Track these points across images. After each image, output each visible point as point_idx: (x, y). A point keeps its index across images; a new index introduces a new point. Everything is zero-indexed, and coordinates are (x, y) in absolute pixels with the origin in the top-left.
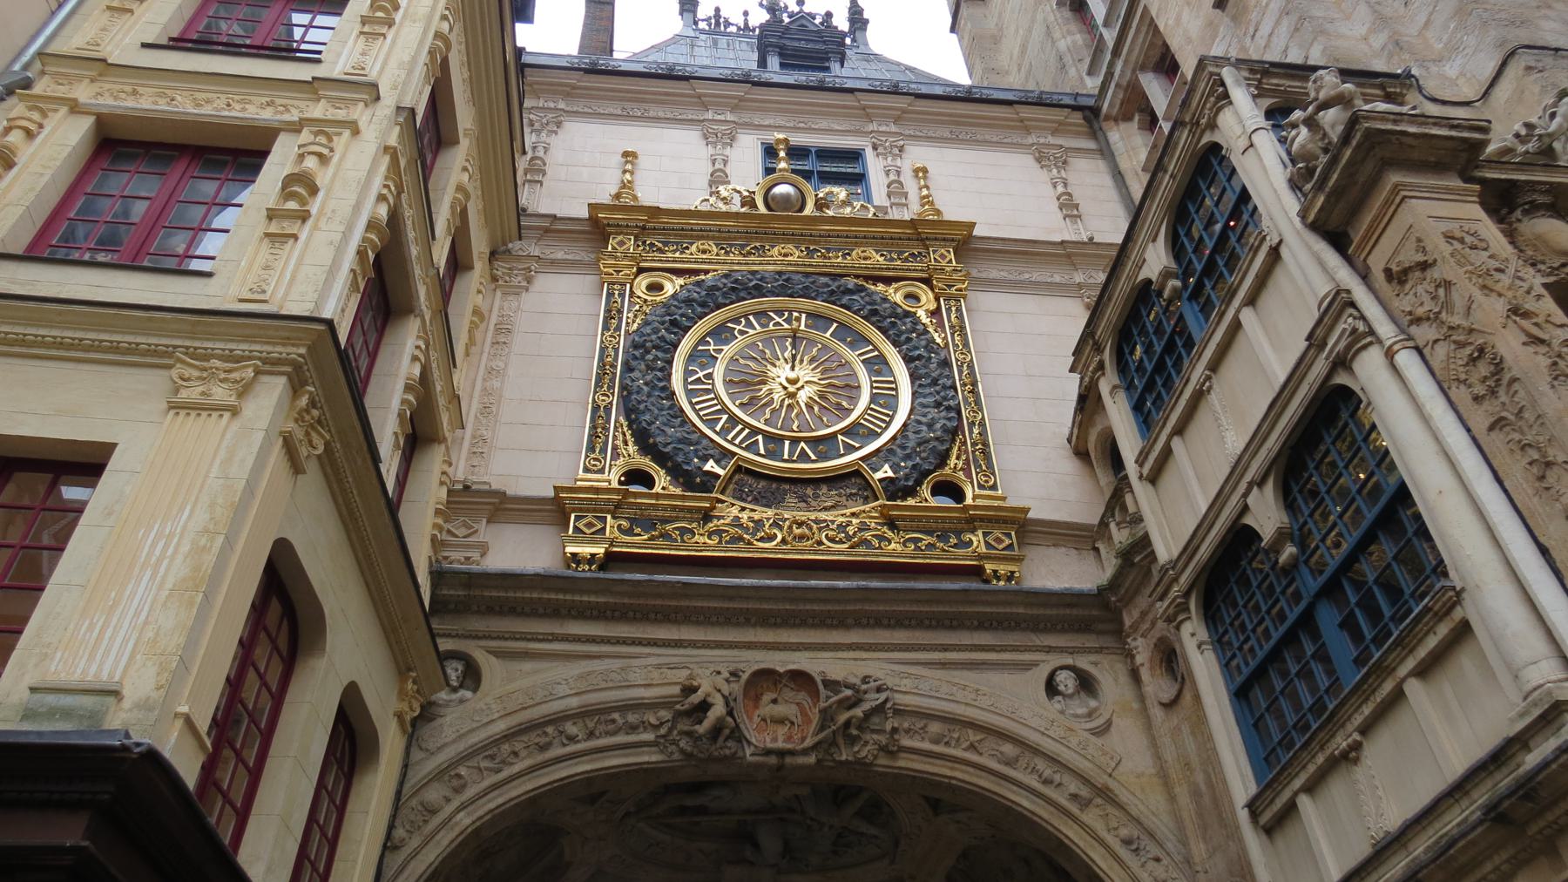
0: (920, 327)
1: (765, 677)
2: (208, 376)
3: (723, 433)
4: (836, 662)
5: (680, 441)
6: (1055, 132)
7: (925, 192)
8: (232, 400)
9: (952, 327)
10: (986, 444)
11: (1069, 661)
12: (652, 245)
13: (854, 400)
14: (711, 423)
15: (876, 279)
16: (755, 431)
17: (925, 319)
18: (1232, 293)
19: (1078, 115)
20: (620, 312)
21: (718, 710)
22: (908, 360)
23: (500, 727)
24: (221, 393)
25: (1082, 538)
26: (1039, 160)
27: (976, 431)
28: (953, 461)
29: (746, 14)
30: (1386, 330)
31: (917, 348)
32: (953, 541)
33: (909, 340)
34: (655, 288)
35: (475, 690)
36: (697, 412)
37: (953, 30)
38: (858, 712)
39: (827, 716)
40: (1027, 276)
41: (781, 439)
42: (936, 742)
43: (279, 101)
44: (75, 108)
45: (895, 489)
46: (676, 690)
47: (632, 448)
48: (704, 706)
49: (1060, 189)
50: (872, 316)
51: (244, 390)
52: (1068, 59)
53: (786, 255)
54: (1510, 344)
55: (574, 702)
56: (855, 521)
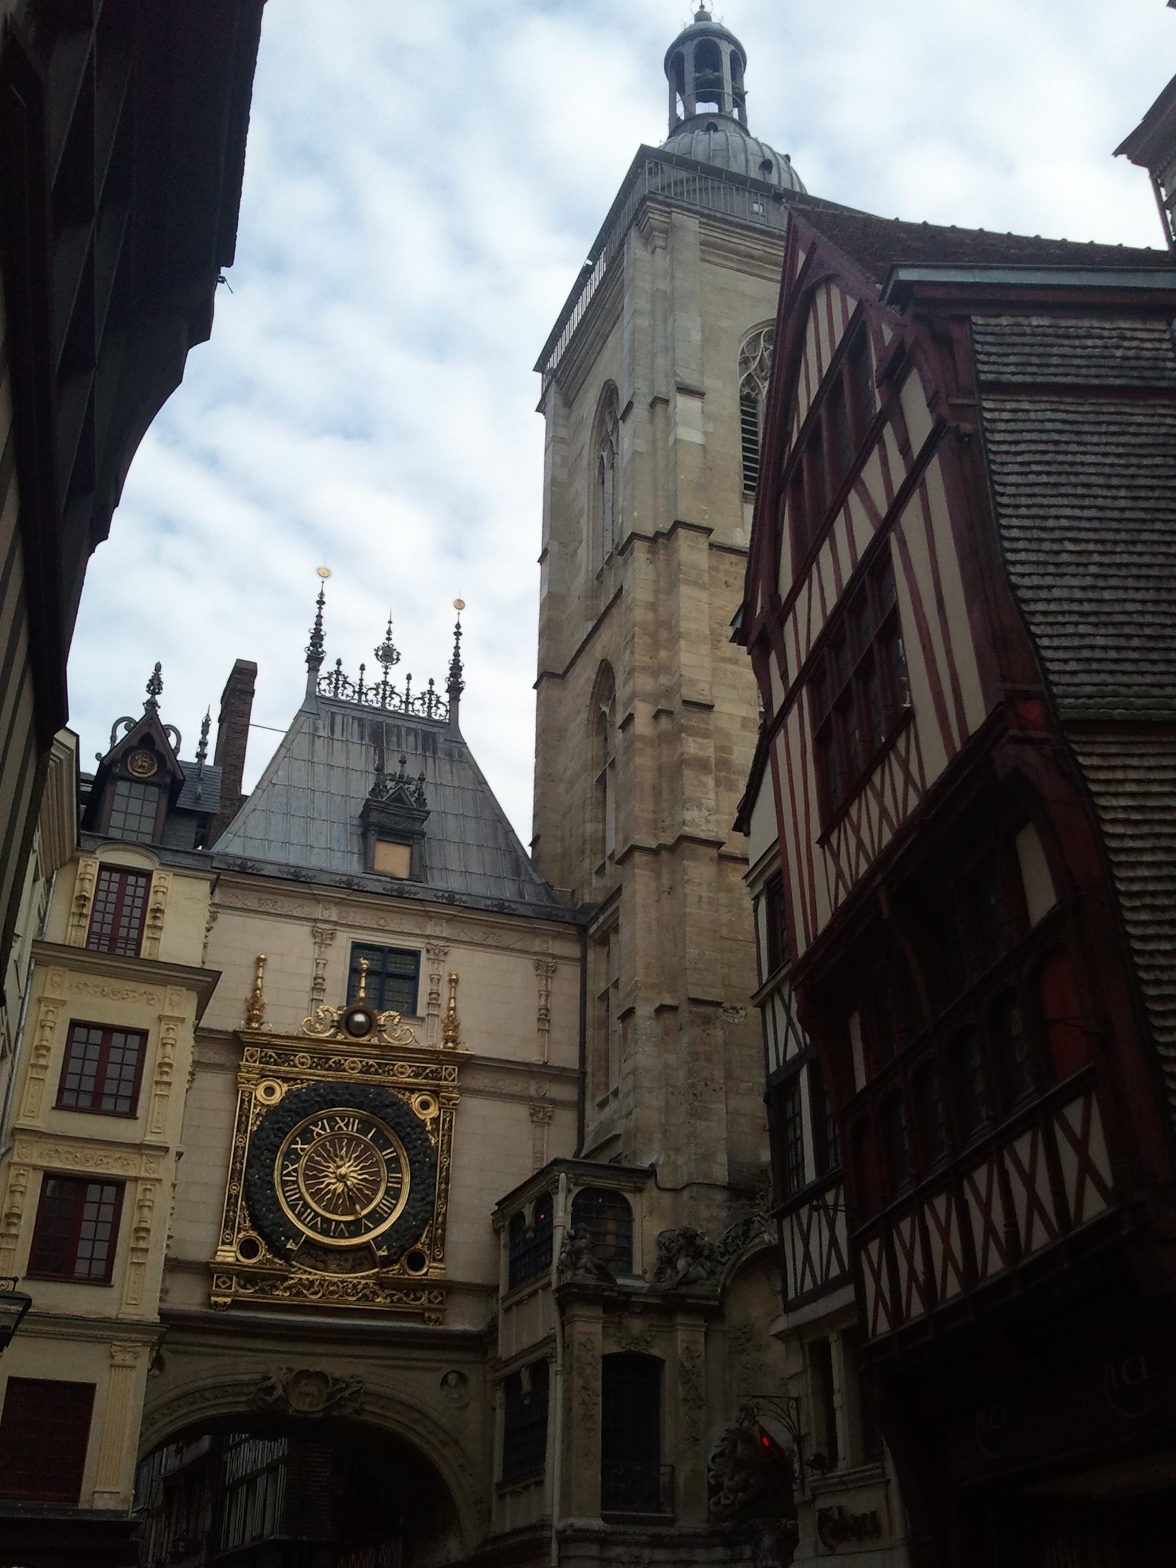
0: (423, 1137)
1: (304, 1374)
2: (124, 1350)
3: (298, 1216)
4: (338, 1365)
5: (274, 1224)
6: (554, 938)
7: (452, 1005)
8: (133, 1363)
9: (443, 1135)
10: (444, 1230)
11: (456, 1368)
12: (271, 1057)
13: (375, 1192)
14: (293, 1208)
15: (406, 1089)
16: (317, 1215)
17: (429, 1128)
18: (537, 1281)
19: (575, 928)
20: (248, 1117)
21: (279, 1391)
22: (412, 1162)
23: (174, 1393)
24: (129, 1359)
25: (486, 1291)
26: (537, 968)
27: (440, 1219)
28: (423, 1239)
29: (362, 668)
30: (559, 1360)
31: (418, 1154)
32: (412, 1296)
33: (415, 1147)
34: (270, 1091)
35: (161, 1370)
36: (286, 1198)
37: (535, 687)
38: (346, 1394)
39: (331, 1396)
40: (502, 1083)
41: (330, 1221)
42: (382, 1408)
43: (124, 1155)
44: (35, 1168)
45: (386, 1262)
46: (258, 1376)
47: (248, 1224)
48: (273, 1388)
49: (543, 1002)
50: (397, 1127)
51: (136, 1356)
52: (588, 846)
53: (353, 1069)
54: (575, 1404)
55: (209, 1381)
56: (363, 1282)
